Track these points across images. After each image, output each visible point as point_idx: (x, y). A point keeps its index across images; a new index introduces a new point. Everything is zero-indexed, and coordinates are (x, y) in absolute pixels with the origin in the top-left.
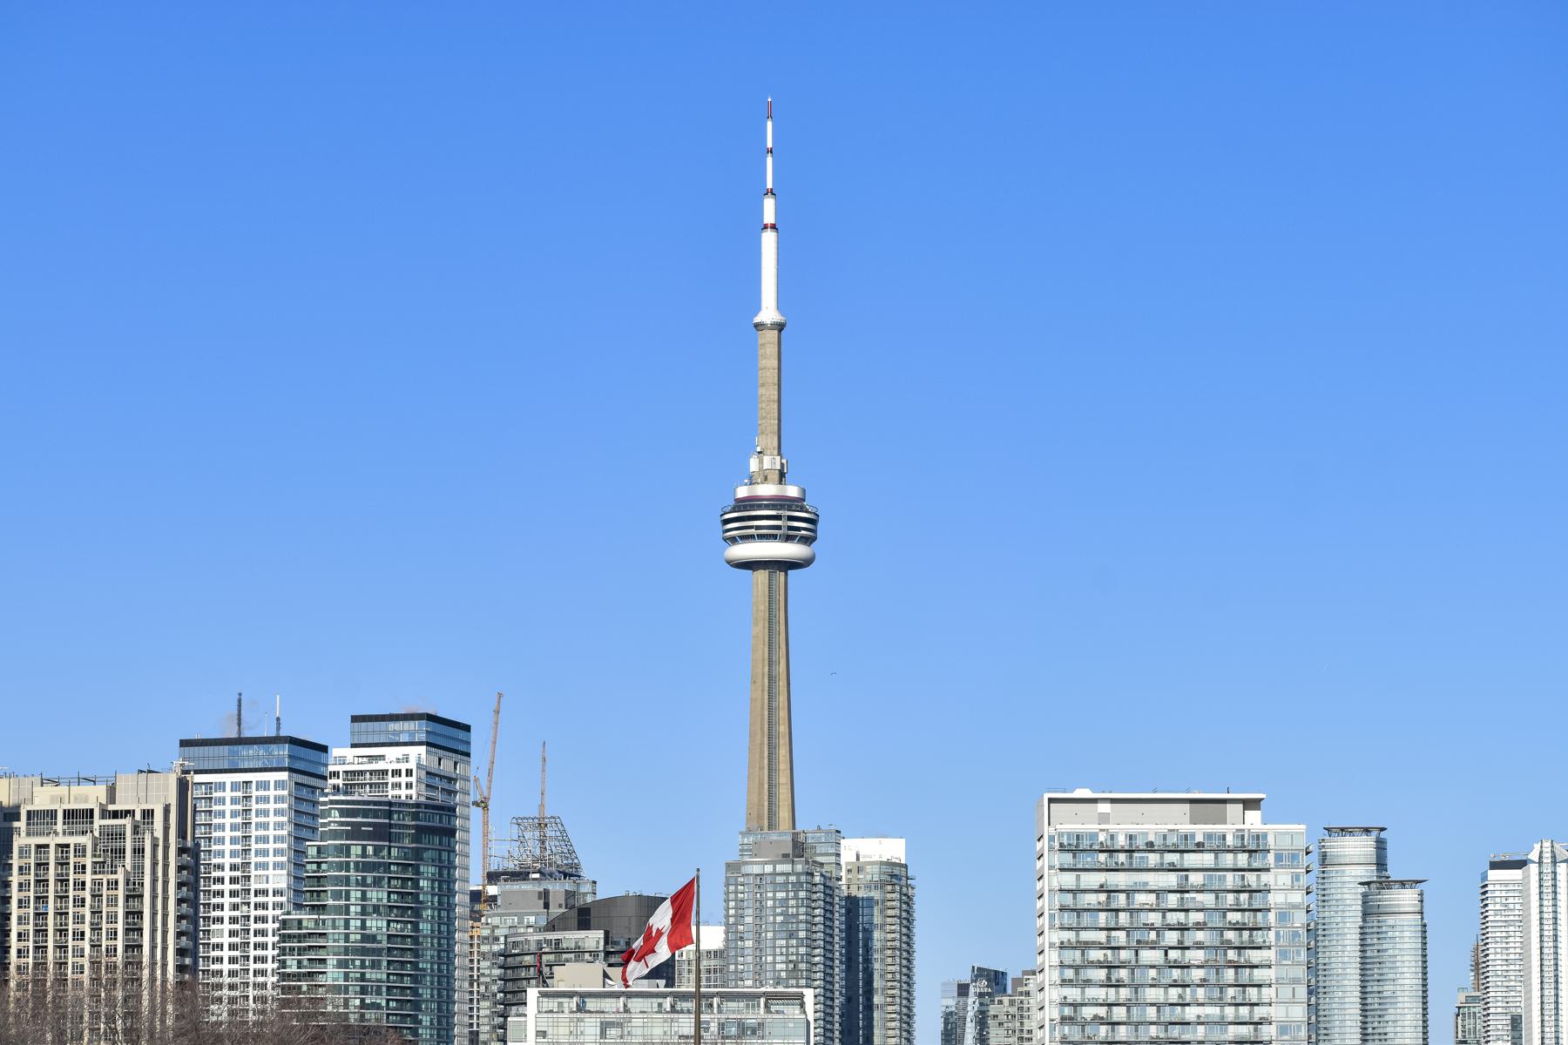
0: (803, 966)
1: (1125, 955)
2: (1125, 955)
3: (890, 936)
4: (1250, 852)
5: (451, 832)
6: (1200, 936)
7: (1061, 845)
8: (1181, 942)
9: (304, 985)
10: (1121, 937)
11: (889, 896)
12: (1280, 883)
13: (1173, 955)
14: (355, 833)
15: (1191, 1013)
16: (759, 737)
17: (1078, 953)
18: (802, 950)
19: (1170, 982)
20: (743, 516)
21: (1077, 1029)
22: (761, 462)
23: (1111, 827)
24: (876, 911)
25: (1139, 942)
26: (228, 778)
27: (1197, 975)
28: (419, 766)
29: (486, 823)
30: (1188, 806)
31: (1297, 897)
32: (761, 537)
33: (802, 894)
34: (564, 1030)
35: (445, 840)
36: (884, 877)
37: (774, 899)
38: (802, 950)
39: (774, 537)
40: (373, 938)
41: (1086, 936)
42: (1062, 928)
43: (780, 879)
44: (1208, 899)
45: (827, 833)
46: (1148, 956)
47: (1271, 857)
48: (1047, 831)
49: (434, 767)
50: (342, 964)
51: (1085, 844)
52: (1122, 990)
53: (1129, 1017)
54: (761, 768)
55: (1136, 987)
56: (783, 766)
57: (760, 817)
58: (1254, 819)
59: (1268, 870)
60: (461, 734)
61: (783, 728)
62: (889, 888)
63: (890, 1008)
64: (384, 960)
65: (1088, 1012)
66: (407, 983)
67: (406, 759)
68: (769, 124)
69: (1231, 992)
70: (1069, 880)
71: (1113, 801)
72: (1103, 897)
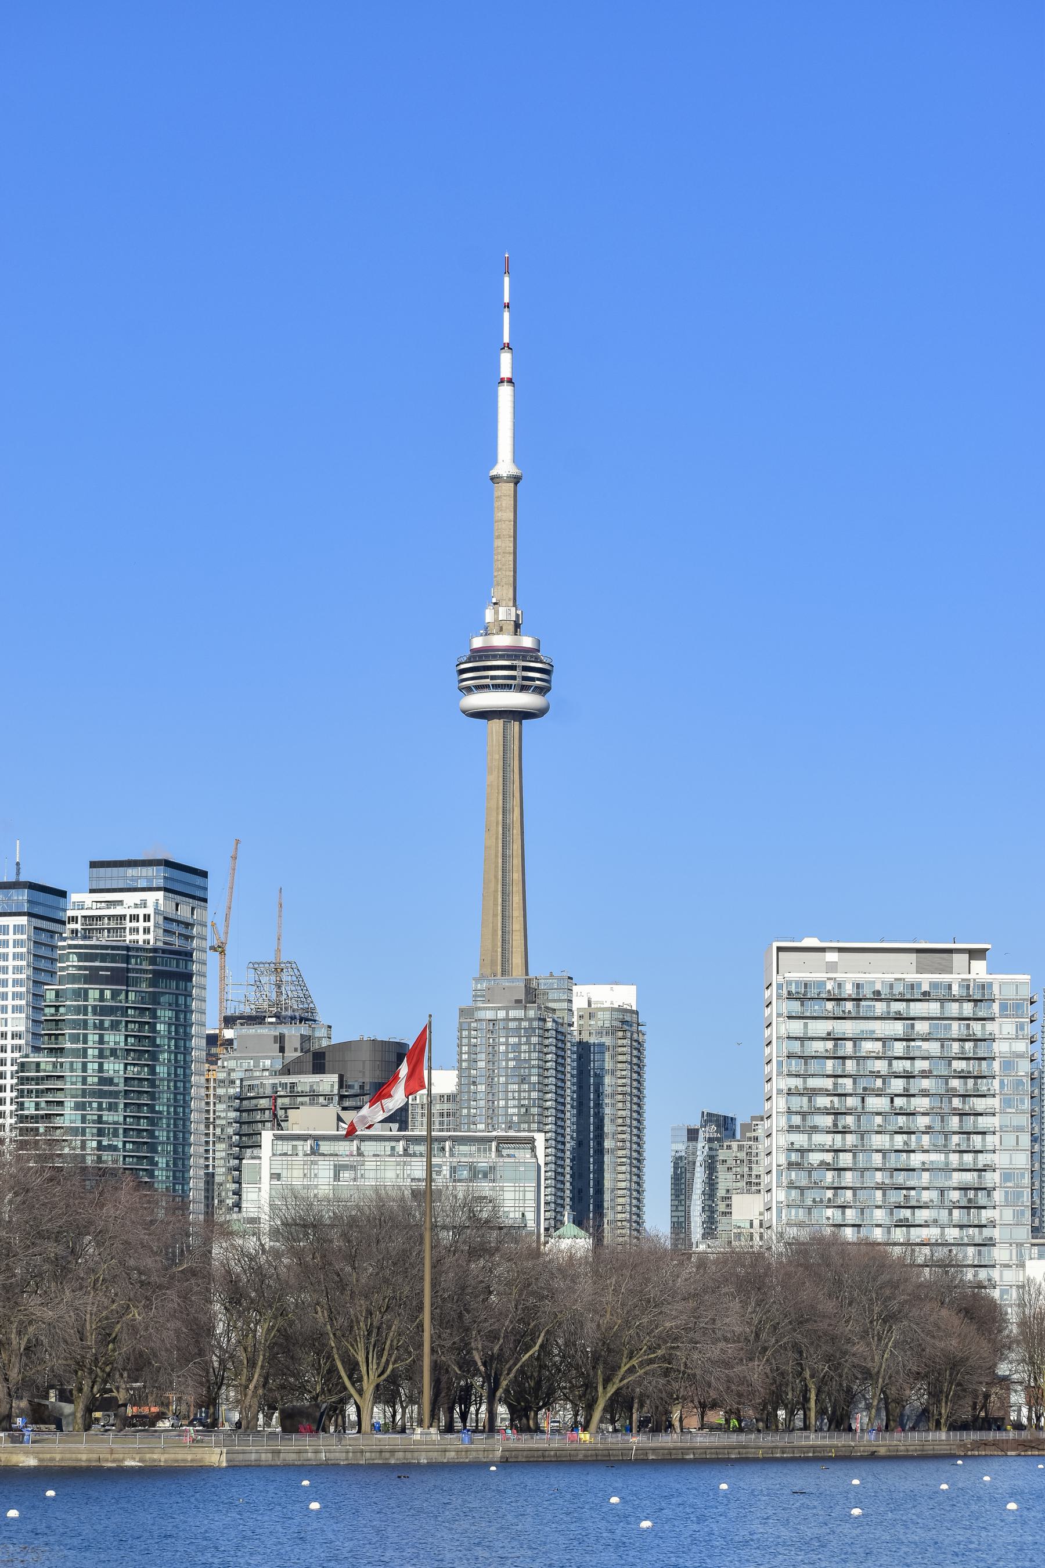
0: (535, 1110)
1: (851, 1102)
2: (851, 1102)
3: (621, 1081)
4: (975, 1001)
5: (188, 977)
6: (925, 1083)
7: (789, 993)
8: (906, 1089)
9: (42, 1127)
10: (847, 1084)
11: (620, 1042)
12: (1005, 1032)
13: (899, 1102)
14: (93, 977)
15: (916, 1160)
16: (492, 885)
17: (805, 1099)
18: (534, 1095)
19: (895, 1128)
20: (479, 668)
21: (804, 1174)
22: (496, 613)
23: (839, 976)
24: (607, 1056)
25: (865, 1089)
27: (922, 1122)
28: (157, 912)
29: (223, 968)
30: (913, 956)
31: (1021, 1046)
32: (496, 687)
33: (534, 1040)
34: (298, 1173)
35: (182, 984)
36: (615, 1023)
37: (507, 1044)
38: (534, 1095)
39: (509, 687)
40: (110, 1081)
41: (813, 1083)
42: (790, 1075)
43: (512, 1025)
44: (933, 1048)
45: (560, 979)
46: (874, 1103)
47: (996, 1007)
48: (775, 979)
49: (171, 913)
50: (79, 1106)
51: (812, 993)
52: (848, 1137)
53: (855, 1163)
54: (495, 915)
55: (862, 1134)
56: (517, 913)
57: (493, 963)
58: (979, 969)
59: (993, 1019)
60: (198, 880)
61: (517, 876)
62: (620, 1034)
63: (621, 1153)
65: (815, 1158)
66: (144, 1125)
67: (144, 904)
68: (507, 280)
69: (955, 1139)
70: (796, 1027)
71: (841, 950)
72: (830, 1045)
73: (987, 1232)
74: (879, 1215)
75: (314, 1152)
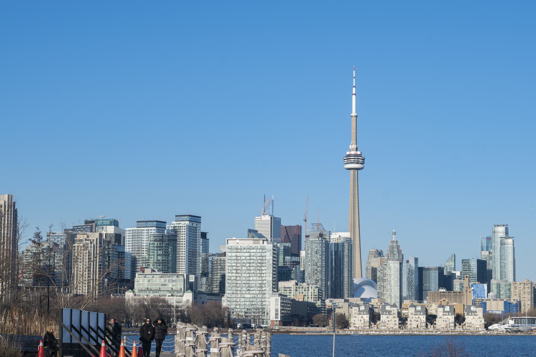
1: (239, 268)
2: (239, 268)
6: (253, 264)
10: (239, 265)
14: (156, 240)
15: (251, 278)
26: (145, 229)
27: (252, 272)
40: (159, 260)
41: (233, 264)
44: (255, 258)
46: (244, 268)
49: (191, 225)
50: (153, 265)
55: (242, 274)
57: (351, 224)
64: (161, 264)
65: (233, 278)
69: (258, 275)
73: (264, 292)
74: (244, 289)
75: (145, 277)
